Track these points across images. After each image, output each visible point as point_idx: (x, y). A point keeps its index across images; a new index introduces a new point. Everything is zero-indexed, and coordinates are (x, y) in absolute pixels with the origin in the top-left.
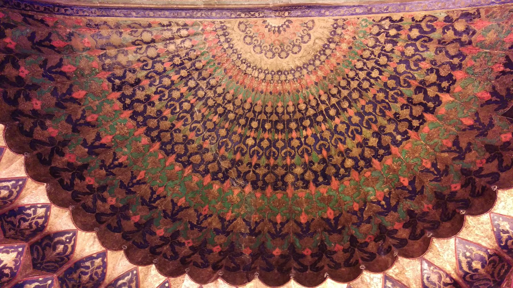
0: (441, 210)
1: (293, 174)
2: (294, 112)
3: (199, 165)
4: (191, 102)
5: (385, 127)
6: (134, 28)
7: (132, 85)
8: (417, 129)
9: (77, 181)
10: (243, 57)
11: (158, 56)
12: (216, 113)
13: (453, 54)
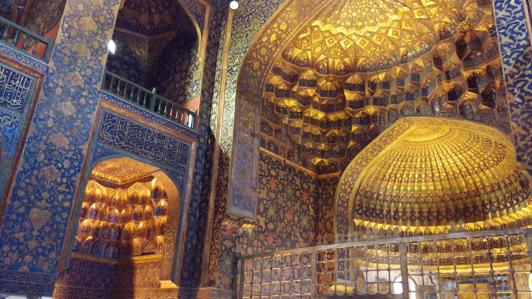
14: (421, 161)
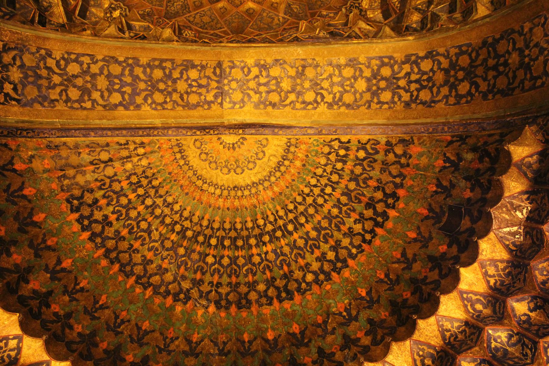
0: (396, 317)
1: (255, 291)
2: (253, 228)
3: (160, 286)
4: (149, 220)
5: (341, 241)
6: (92, 147)
7: (90, 206)
8: (370, 242)
9: (44, 309)
10: (199, 172)
11: (116, 175)
12: (173, 230)
13: (395, 174)
14: (182, 233)
